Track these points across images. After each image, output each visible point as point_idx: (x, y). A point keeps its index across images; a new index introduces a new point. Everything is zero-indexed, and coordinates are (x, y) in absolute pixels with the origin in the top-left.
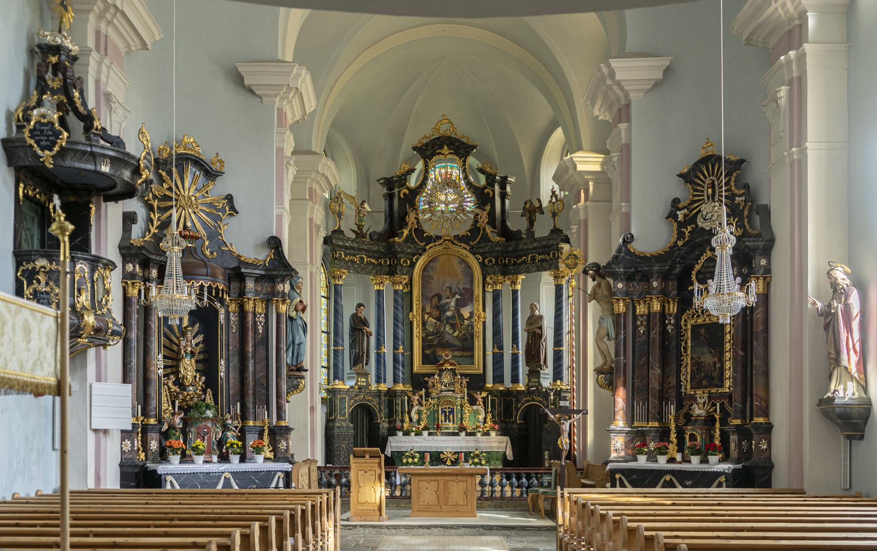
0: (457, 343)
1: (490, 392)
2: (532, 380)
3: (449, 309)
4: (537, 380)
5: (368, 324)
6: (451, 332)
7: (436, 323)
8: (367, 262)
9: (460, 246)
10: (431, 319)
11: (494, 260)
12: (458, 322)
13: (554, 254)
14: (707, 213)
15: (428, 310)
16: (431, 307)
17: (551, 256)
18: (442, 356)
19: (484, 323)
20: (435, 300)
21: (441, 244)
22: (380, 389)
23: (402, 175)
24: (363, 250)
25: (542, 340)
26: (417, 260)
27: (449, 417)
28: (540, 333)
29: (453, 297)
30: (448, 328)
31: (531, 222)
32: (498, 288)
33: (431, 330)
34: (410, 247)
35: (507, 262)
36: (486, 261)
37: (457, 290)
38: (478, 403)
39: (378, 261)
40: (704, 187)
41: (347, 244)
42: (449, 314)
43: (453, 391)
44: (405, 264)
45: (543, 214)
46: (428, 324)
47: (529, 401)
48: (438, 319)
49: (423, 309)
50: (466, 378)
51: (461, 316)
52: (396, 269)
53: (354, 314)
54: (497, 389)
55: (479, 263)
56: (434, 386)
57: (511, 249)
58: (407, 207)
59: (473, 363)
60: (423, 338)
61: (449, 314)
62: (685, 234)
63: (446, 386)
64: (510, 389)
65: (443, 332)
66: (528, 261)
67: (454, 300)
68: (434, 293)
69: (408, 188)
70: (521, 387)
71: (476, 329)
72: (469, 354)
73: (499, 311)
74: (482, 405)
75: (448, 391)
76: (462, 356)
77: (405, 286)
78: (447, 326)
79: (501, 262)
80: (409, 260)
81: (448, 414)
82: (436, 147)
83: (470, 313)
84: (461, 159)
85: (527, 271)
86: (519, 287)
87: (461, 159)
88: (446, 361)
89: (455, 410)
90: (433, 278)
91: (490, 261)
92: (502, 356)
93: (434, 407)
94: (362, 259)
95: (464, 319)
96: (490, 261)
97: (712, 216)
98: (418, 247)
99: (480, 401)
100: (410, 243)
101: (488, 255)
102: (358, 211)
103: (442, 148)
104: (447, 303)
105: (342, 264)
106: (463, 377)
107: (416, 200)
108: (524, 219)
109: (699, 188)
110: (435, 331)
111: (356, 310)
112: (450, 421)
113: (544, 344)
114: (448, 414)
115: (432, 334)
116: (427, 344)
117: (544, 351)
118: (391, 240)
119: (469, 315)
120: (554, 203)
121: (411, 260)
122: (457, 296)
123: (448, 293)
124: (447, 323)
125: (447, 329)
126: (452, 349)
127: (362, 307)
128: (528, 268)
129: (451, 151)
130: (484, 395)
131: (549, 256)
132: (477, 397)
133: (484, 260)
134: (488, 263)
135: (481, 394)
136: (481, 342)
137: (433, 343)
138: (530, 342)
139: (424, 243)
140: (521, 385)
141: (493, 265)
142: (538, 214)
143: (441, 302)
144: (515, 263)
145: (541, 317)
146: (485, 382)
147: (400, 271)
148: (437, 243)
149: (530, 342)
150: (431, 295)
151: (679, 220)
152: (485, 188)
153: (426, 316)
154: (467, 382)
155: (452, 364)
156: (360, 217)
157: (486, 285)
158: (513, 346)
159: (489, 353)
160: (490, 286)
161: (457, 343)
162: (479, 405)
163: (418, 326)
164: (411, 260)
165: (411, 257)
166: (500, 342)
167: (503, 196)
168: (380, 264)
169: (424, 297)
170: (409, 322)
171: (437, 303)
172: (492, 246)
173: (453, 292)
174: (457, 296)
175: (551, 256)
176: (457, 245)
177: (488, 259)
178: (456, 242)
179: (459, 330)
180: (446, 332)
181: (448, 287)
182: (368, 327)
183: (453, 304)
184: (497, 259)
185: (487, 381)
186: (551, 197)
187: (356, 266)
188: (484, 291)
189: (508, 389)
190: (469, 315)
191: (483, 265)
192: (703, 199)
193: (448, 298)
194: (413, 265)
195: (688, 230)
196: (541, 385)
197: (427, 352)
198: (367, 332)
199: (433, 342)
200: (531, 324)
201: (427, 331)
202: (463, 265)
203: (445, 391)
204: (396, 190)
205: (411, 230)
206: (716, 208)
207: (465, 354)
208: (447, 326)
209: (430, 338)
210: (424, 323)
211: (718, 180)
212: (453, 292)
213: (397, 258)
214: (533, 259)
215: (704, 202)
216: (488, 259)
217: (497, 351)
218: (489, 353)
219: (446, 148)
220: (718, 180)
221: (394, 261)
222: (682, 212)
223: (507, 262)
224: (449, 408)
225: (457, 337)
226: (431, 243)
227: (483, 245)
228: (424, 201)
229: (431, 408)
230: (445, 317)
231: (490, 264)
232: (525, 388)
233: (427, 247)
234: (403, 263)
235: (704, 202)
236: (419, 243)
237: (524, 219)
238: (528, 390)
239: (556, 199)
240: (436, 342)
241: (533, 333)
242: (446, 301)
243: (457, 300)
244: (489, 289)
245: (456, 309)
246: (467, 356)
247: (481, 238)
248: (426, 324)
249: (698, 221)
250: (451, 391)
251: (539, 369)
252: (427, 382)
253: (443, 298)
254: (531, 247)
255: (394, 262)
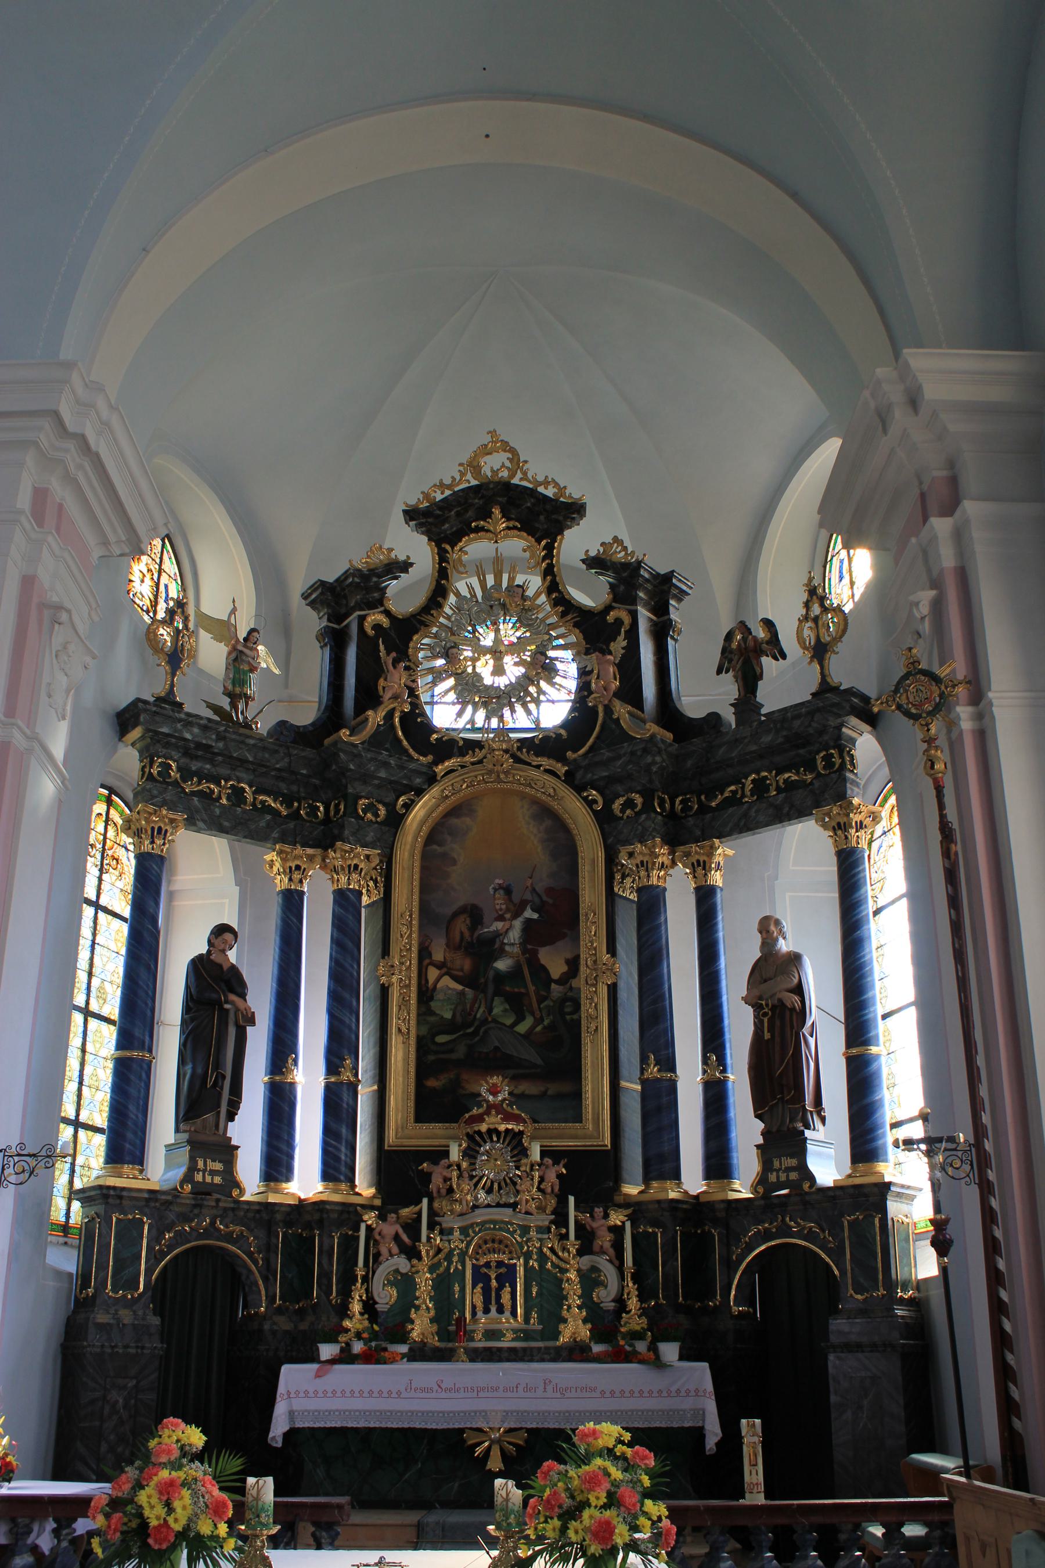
0: (530, 1055)
1: (637, 1210)
2: (776, 1164)
3: (501, 953)
4: (793, 1162)
5: (243, 984)
6: (509, 1022)
7: (462, 994)
8: (254, 804)
9: (538, 767)
10: (447, 982)
11: (639, 800)
12: (532, 988)
13: (828, 758)
15: (438, 956)
16: (448, 945)
17: (820, 764)
18: (480, 1095)
19: (613, 989)
20: (462, 925)
21: (480, 762)
22: (272, 1198)
23: (372, 572)
24: (243, 761)
25: (806, 1030)
26: (408, 806)
27: (498, 1297)
28: (798, 1005)
29: (515, 916)
30: (499, 1007)
31: (749, 679)
32: (654, 881)
33: (448, 1015)
34: (386, 765)
35: (678, 807)
36: (617, 806)
37: (528, 896)
38: (596, 1248)
39: (289, 805)
41: (188, 736)
42: (502, 965)
43: (514, 1206)
44: (369, 815)
45: (784, 656)
46: (439, 996)
47: (767, 1236)
48: (469, 981)
49: (424, 953)
50: (556, 1162)
51: (540, 973)
52: (342, 827)
53: (201, 955)
54: (661, 1196)
55: (595, 812)
56: (450, 1191)
57: (689, 763)
58: (382, 647)
59: (578, 1118)
60: (420, 1040)
61: (502, 965)
63: (489, 1191)
64: (702, 1199)
65: (484, 1022)
66: (743, 796)
67: (518, 924)
68: (455, 907)
69: (387, 613)
70: (741, 1189)
71: (586, 1009)
72: (566, 1088)
73: (660, 950)
74: (611, 1251)
75: (498, 1205)
76: (543, 1095)
77: (371, 884)
78: (497, 1001)
79: (662, 806)
80: (384, 804)
81: (494, 1283)
82: (470, 514)
83: (568, 962)
84: (539, 541)
85: (747, 825)
86: (717, 878)
87: (539, 541)
88: (491, 1107)
89: (521, 1271)
90: (454, 862)
91: (629, 804)
92: (672, 1089)
93: (450, 1263)
94: (237, 795)
95: (548, 980)
96: (629, 804)
98: (412, 766)
99: (605, 1240)
100: (387, 750)
101: (619, 788)
102: (234, 655)
103: (487, 515)
104: (497, 935)
105: (168, 796)
106: (548, 1161)
107: (411, 645)
108: (728, 677)
110: (459, 1019)
111: (209, 942)
112: (500, 1310)
113: (812, 1041)
114: (494, 1283)
115: (450, 1027)
116: (431, 1058)
117: (812, 1064)
118: (327, 742)
119: (564, 968)
120: (816, 620)
121: (391, 807)
122: (529, 914)
123: (500, 902)
124: (497, 993)
125: (496, 1011)
126: (511, 1072)
127: (229, 936)
128: (745, 815)
129: (511, 524)
130: (616, 1218)
131: (811, 766)
132: (595, 1225)
133: (608, 803)
134: (623, 811)
135: (606, 1216)
136: (606, 1047)
137: (454, 1056)
138: (767, 1036)
139: (430, 758)
140: (737, 1184)
141: (638, 814)
142: (766, 661)
143: (476, 935)
144: (703, 809)
145: (795, 959)
146: (618, 1180)
147: (354, 834)
148: (468, 759)
149: (767, 1036)
150: (449, 911)
152: (608, 609)
153: (433, 973)
154: (560, 1176)
155: (508, 1117)
156: (237, 671)
157: (618, 877)
158: (705, 1061)
159: (632, 1086)
160: (628, 881)
161: (530, 1055)
162: (602, 1252)
163: (404, 1002)
164: (391, 807)
165: (389, 798)
166: (667, 1048)
167: (662, 632)
168: (295, 815)
169: (426, 913)
170: (378, 991)
171: (467, 934)
172: (633, 753)
173: (516, 898)
174: (529, 914)
175: (820, 764)
176: (529, 764)
177: (621, 800)
178: (524, 756)
179: (533, 1014)
180: (495, 1021)
181: (501, 887)
182: (243, 996)
183: (515, 935)
184: (648, 795)
185: (625, 1175)
186: (807, 605)
187: (217, 811)
188: (611, 896)
189: (697, 1197)
190: (564, 968)
191: (604, 819)
193: (501, 918)
194: (395, 820)
196: (811, 1178)
197: (432, 1083)
198: (237, 1010)
199: (452, 1051)
200: (765, 981)
201: (432, 1019)
202: (548, 823)
203: (488, 1206)
204: (353, 619)
205: (390, 715)
207: (553, 1088)
208: (497, 1001)
209: (441, 1039)
210: (426, 995)
212: (516, 898)
213: (345, 797)
214: (760, 787)
216: (621, 800)
217: (653, 1071)
218: (632, 1086)
219: (497, 512)
221: (337, 806)
223: (678, 807)
224: (500, 1264)
225: (527, 1036)
226: (449, 757)
227: (606, 754)
228: (430, 647)
229: (439, 1264)
230: (491, 974)
231: (628, 812)
232: (754, 1189)
233: (440, 769)
234: (365, 811)
236: (416, 756)
237: (728, 677)
238: (766, 1196)
239: (822, 605)
240: (461, 1052)
241: (774, 1008)
242: (493, 928)
243: (528, 923)
244: (628, 892)
245: (524, 951)
246: (560, 1096)
247: (598, 738)
248: (431, 998)
250: (506, 1205)
251: (800, 1126)
252: (427, 1177)
253: (486, 919)
254: (754, 748)
255: (337, 811)
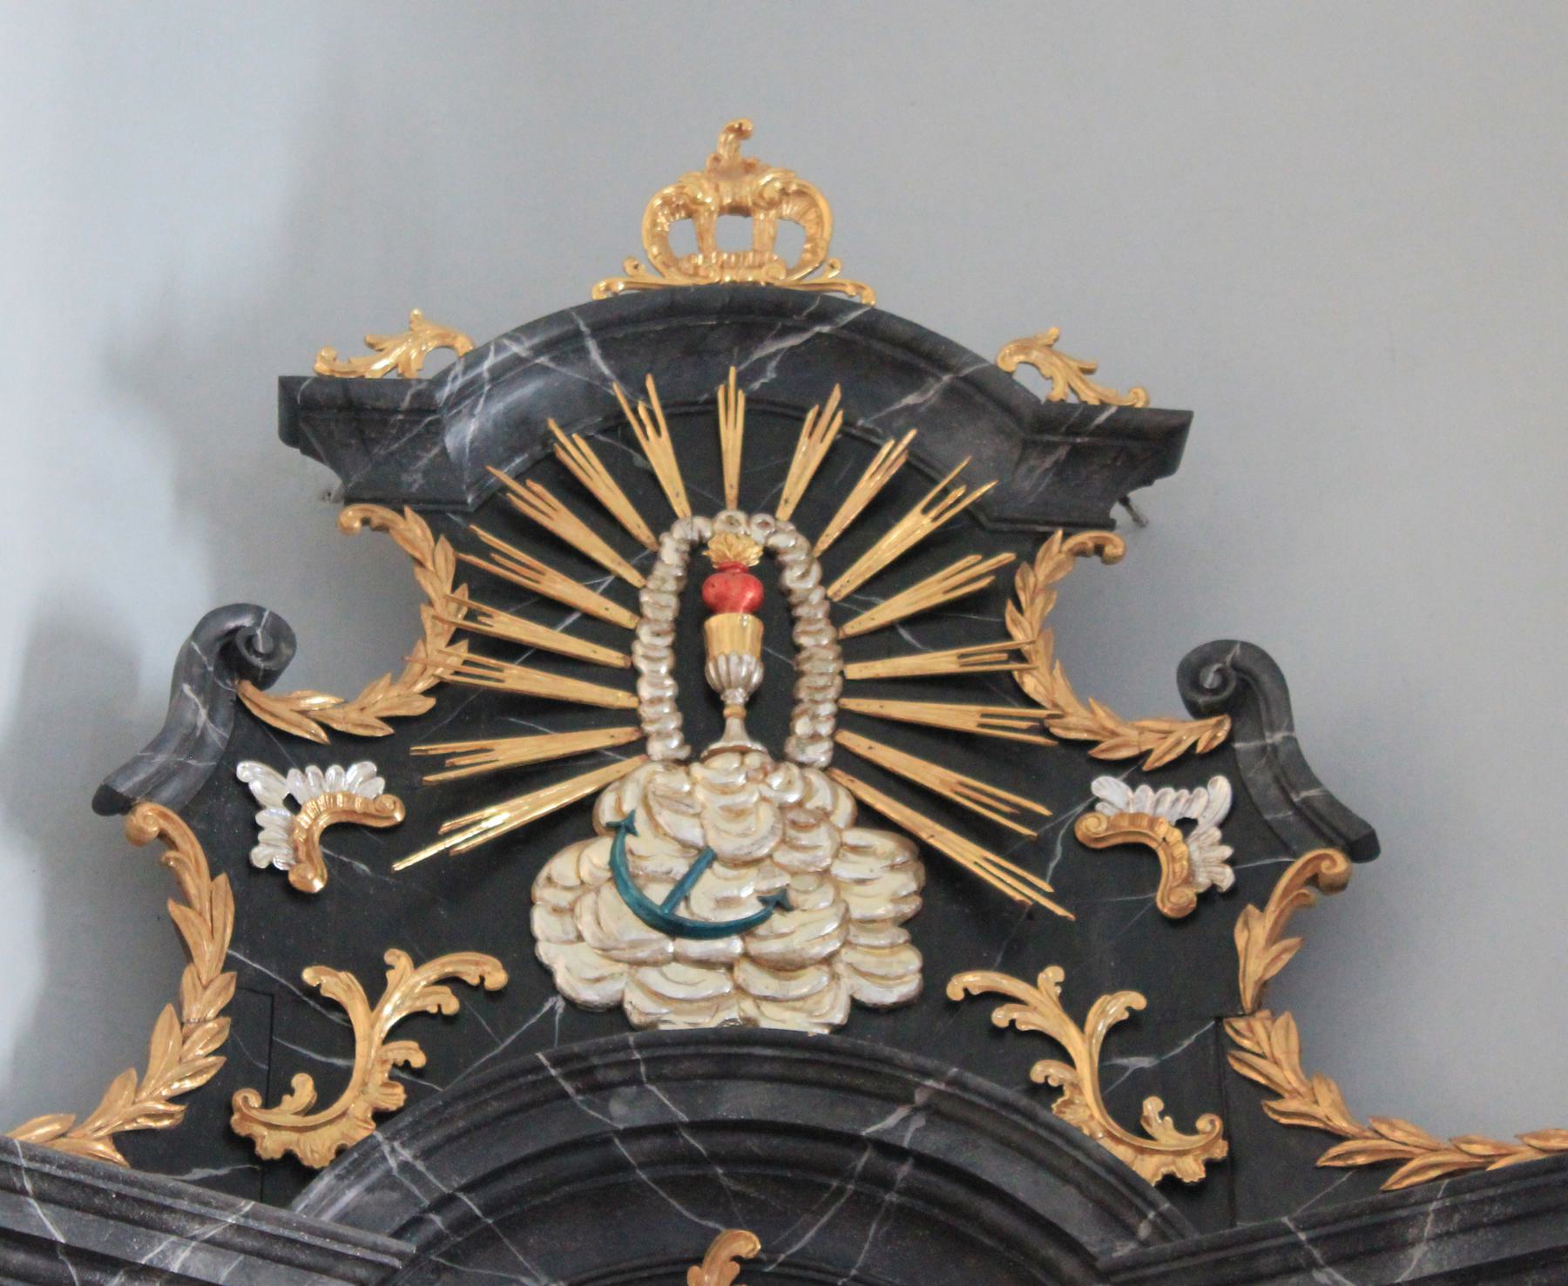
14: (705, 858)
40: (626, 595)
62: (345, 1039)
97: (778, 902)
109: (558, 585)
151: (261, 856)
192: (629, 717)
195: (391, 1011)
206: (821, 838)
211: (833, 563)
215: (637, 747)
220: (833, 563)
222: (296, 782)
235: (637, 747)
249: (541, 922)
